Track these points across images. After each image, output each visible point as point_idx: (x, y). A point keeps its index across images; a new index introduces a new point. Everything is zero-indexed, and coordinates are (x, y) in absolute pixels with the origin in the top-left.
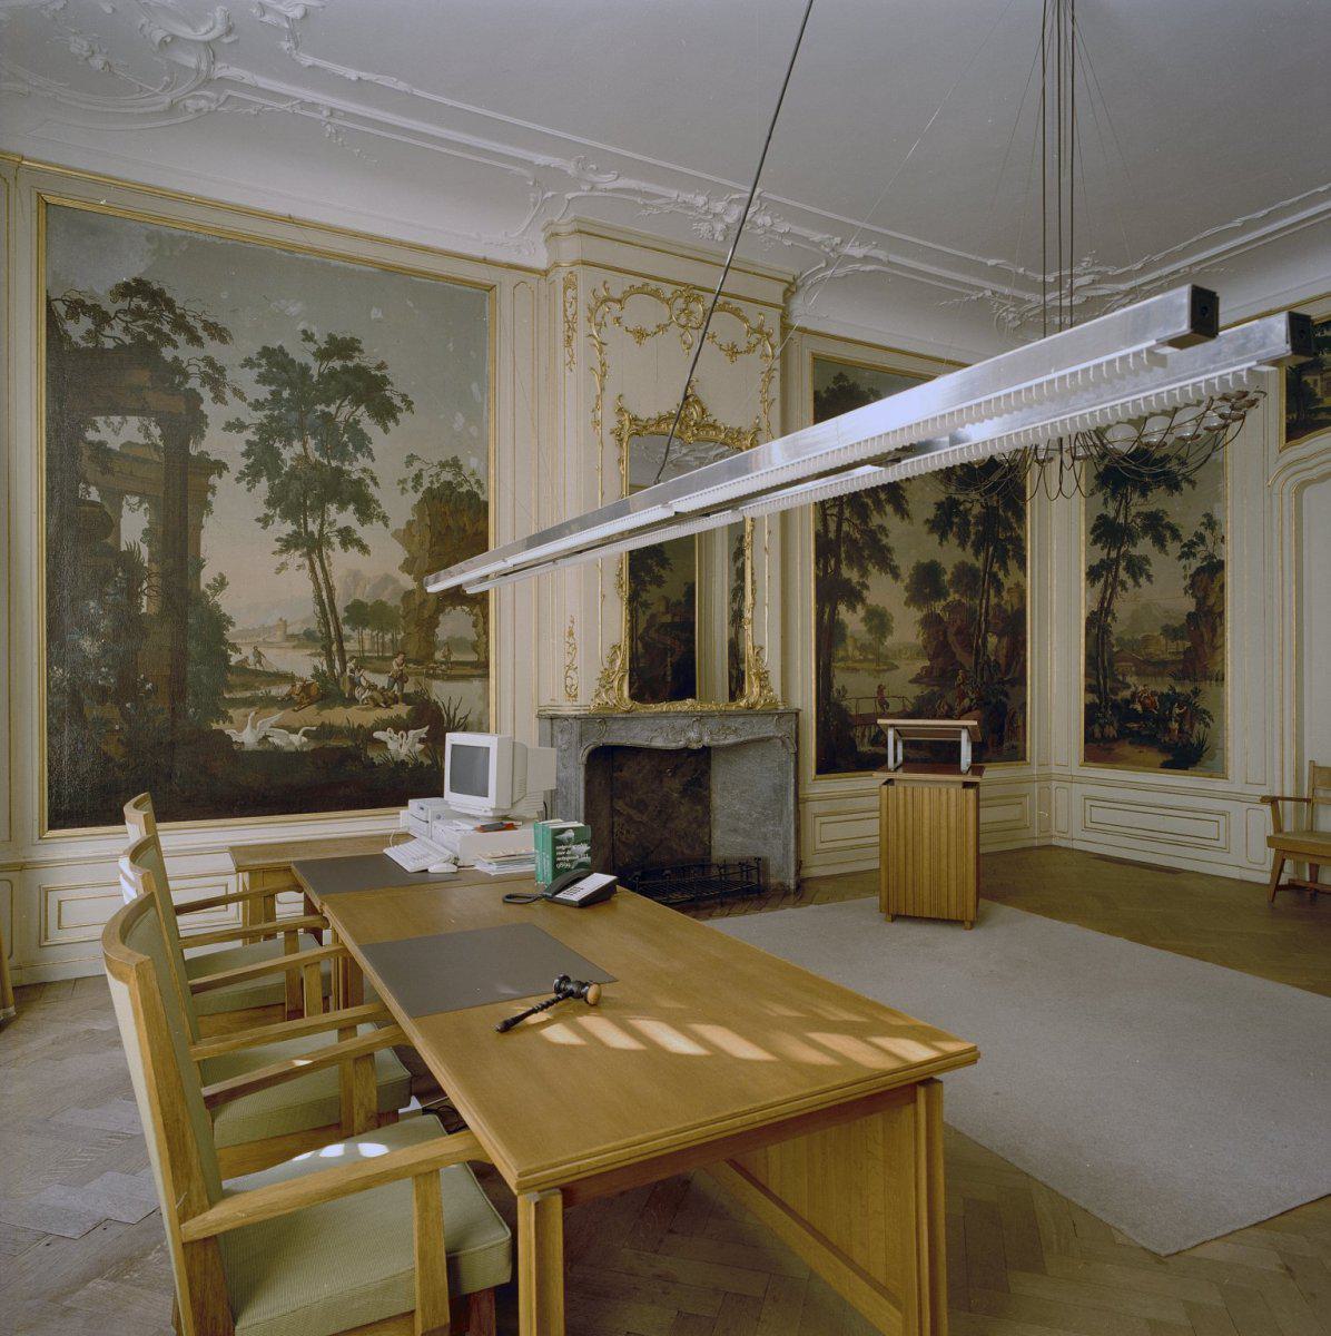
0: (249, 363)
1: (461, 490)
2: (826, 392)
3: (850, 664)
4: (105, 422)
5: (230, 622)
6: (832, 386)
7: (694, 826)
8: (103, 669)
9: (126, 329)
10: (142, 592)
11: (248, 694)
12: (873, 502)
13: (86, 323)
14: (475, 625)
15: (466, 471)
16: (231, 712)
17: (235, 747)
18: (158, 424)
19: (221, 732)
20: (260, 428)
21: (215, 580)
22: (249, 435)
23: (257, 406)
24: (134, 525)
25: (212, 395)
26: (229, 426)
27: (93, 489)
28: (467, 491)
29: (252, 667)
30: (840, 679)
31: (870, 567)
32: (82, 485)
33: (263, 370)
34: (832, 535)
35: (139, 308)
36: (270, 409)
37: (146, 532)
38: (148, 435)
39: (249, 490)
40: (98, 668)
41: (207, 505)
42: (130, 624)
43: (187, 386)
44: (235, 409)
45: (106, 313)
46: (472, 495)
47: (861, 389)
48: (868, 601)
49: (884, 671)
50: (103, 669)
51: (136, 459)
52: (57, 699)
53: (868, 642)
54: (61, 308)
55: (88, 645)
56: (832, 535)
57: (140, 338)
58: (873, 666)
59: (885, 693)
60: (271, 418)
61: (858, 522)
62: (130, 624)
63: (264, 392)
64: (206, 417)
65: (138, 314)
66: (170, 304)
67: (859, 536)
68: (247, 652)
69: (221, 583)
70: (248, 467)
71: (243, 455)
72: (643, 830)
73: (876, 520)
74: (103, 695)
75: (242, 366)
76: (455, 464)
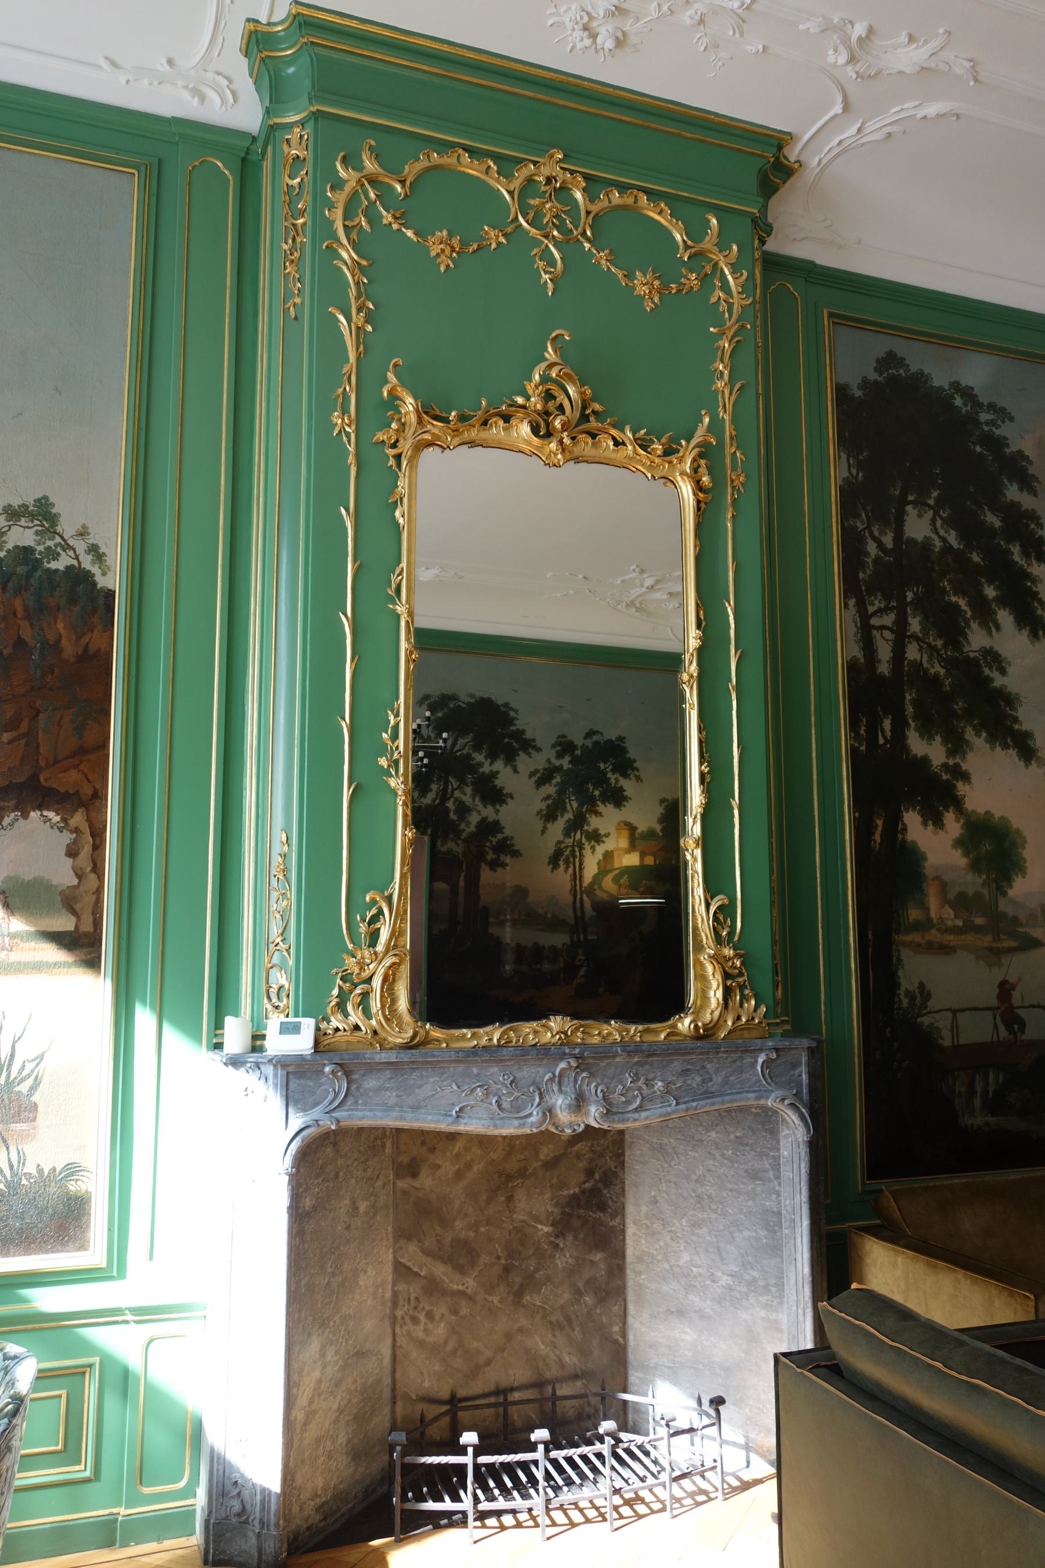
1: (53, 565)
2: (859, 388)
3: (934, 935)
6: (874, 376)
7: (589, 1299)
12: (970, 604)
14: (72, 852)
15: (67, 527)
28: (67, 568)
30: (916, 969)
31: (969, 734)
34: (884, 668)
46: (78, 577)
47: (936, 383)
48: (970, 805)
49: (1010, 950)
53: (970, 892)
56: (884, 668)
58: (987, 940)
59: (1016, 999)
61: (939, 643)
67: (942, 671)
72: (465, 1311)
73: (977, 639)
76: (43, 513)
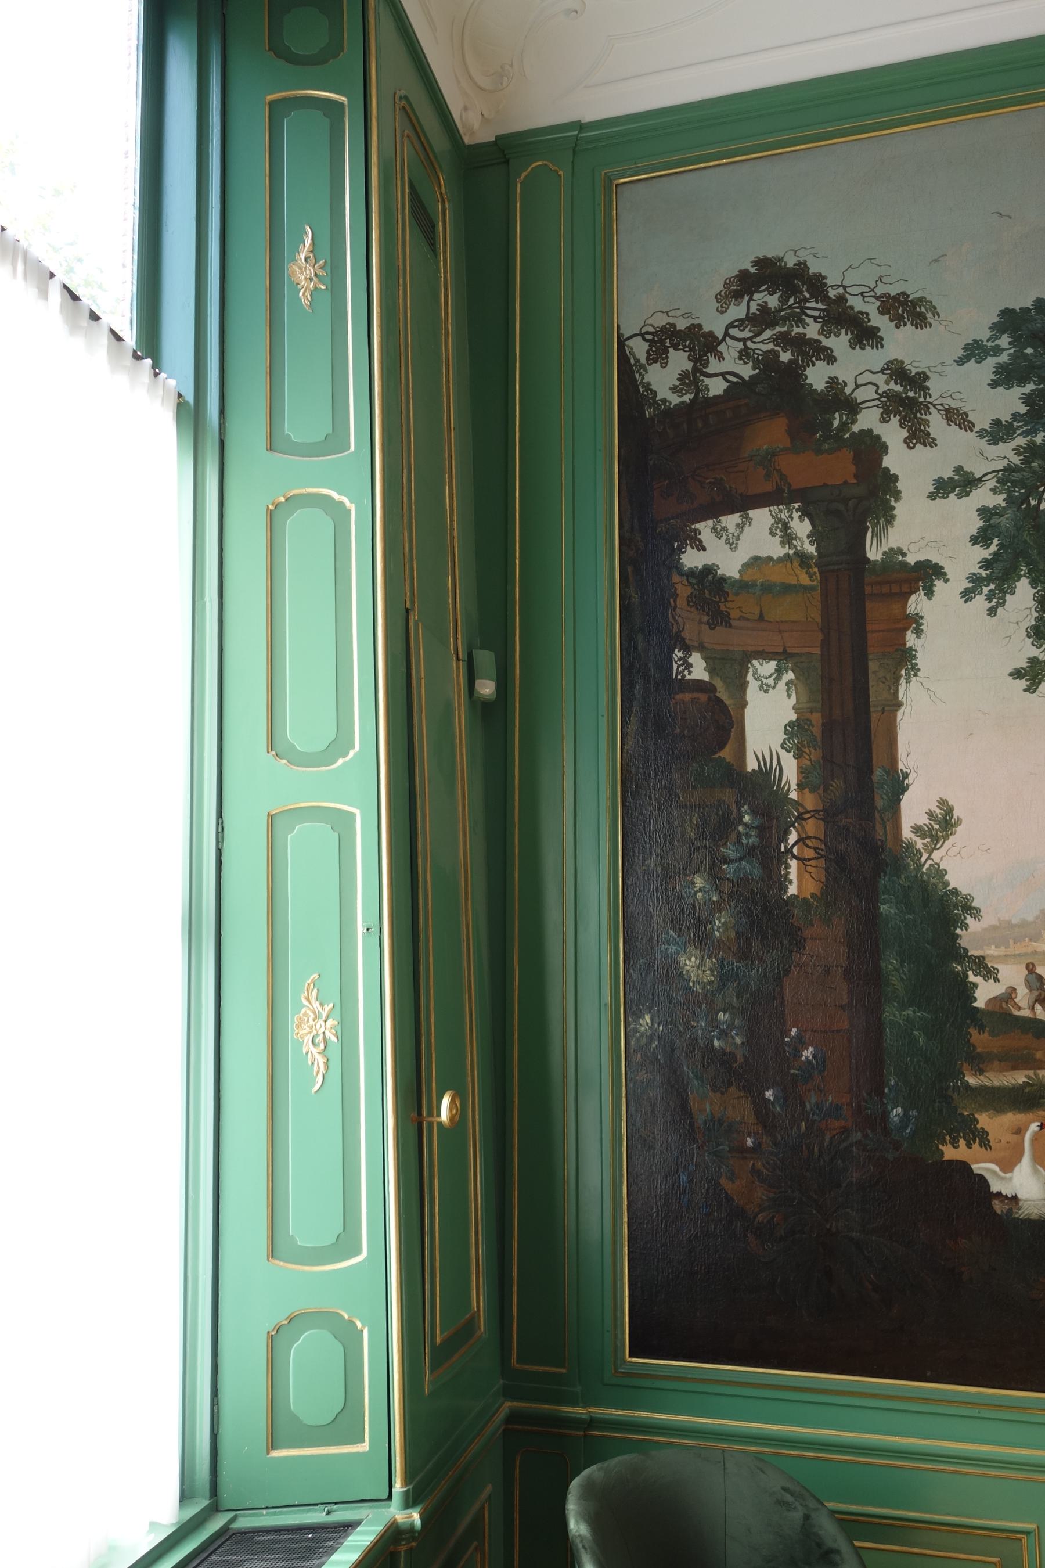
0: (974, 351)
4: (714, 529)
5: (969, 908)
8: (721, 1016)
9: (745, 354)
10: (789, 851)
11: (1020, 1078)
13: (679, 361)
16: (984, 1120)
17: (998, 1206)
18: (805, 513)
19: (964, 1167)
20: (1007, 477)
21: (931, 814)
22: (986, 496)
23: (998, 432)
24: (769, 716)
25: (905, 433)
26: (942, 488)
27: (697, 660)
29: (1026, 1013)
32: (678, 654)
33: (1004, 358)
35: (764, 308)
36: (1025, 434)
37: (794, 730)
38: (788, 538)
39: (992, 612)
40: (712, 1012)
41: (903, 659)
42: (767, 919)
43: (856, 428)
44: (955, 448)
45: (711, 334)
50: (721, 1016)
51: (767, 588)
52: (642, 1076)
54: (639, 349)
55: (694, 966)
57: (768, 363)
60: (1031, 452)
62: (767, 919)
63: (1010, 402)
64: (895, 478)
65: (762, 319)
66: (817, 285)
68: (1012, 976)
69: (944, 823)
70: (986, 564)
71: (974, 540)
74: (726, 1071)
75: (961, 362)
